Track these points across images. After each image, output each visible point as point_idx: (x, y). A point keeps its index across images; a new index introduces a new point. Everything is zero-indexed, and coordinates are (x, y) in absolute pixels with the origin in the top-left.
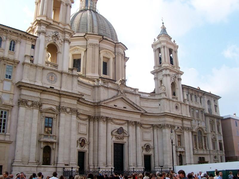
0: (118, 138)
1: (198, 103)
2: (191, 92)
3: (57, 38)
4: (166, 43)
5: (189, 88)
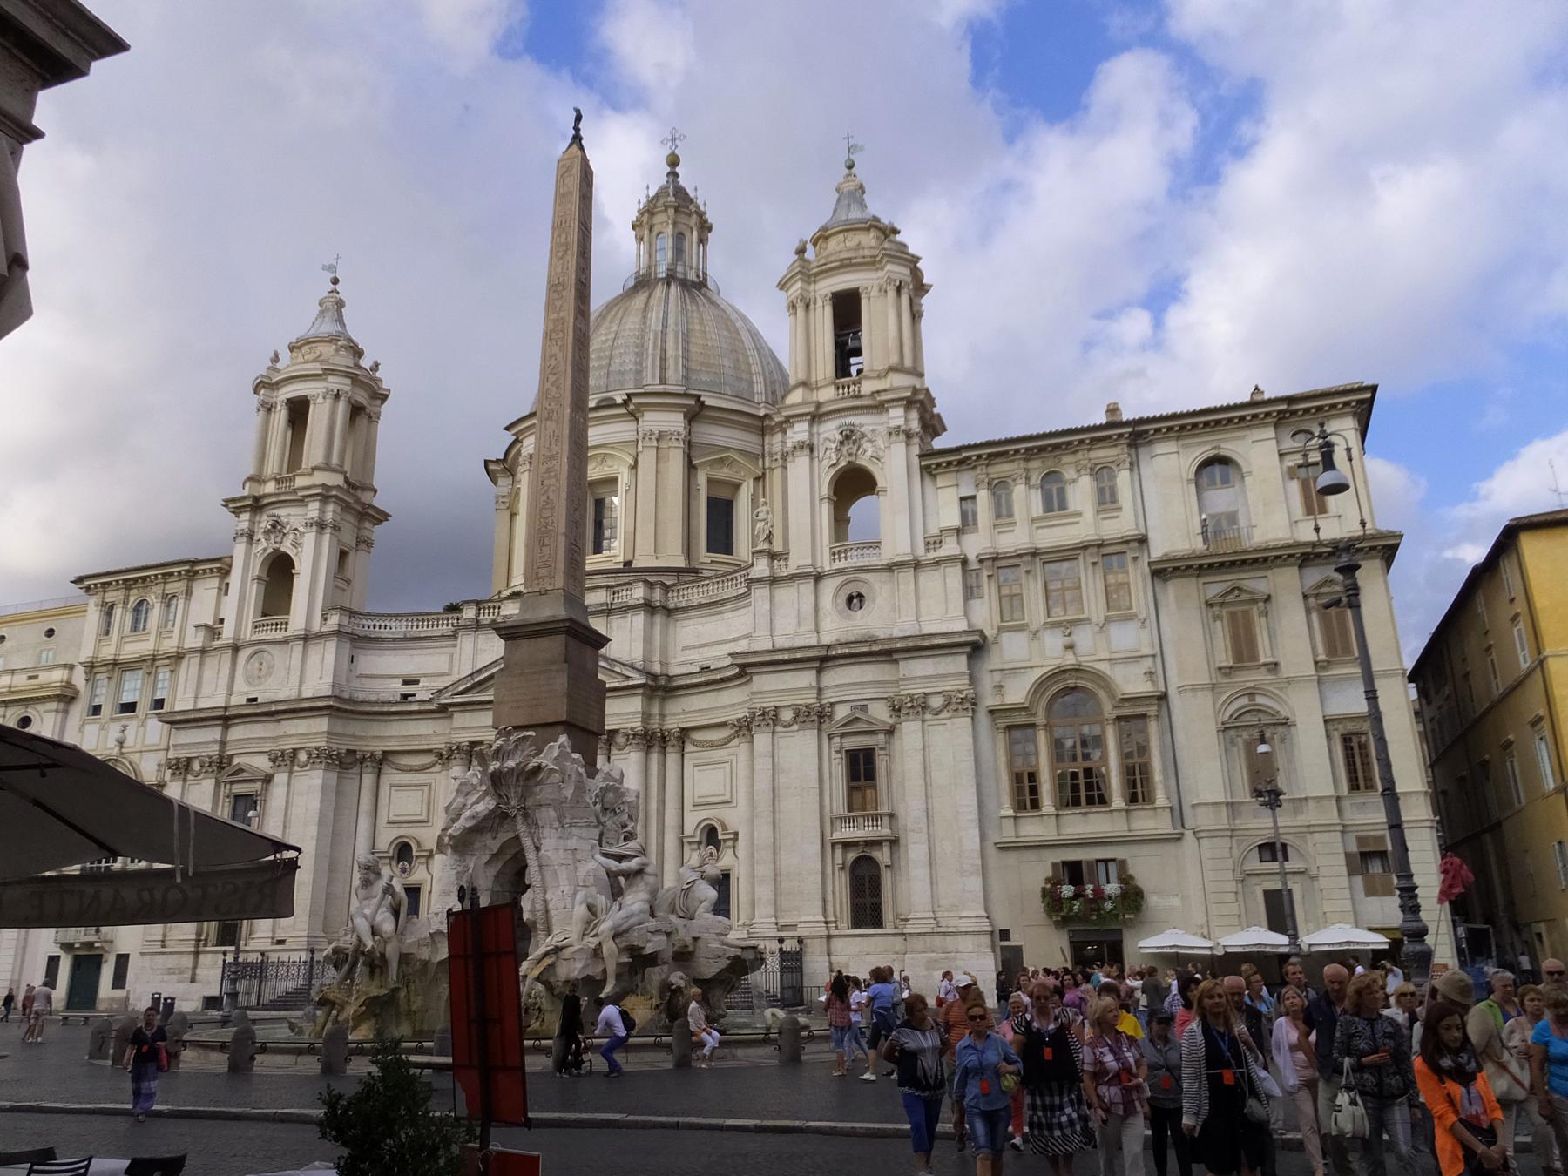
1: (1079, 514)
2: (1001, 469)
3: (280, 531)
4: (799, 284)
5: (969, 458)
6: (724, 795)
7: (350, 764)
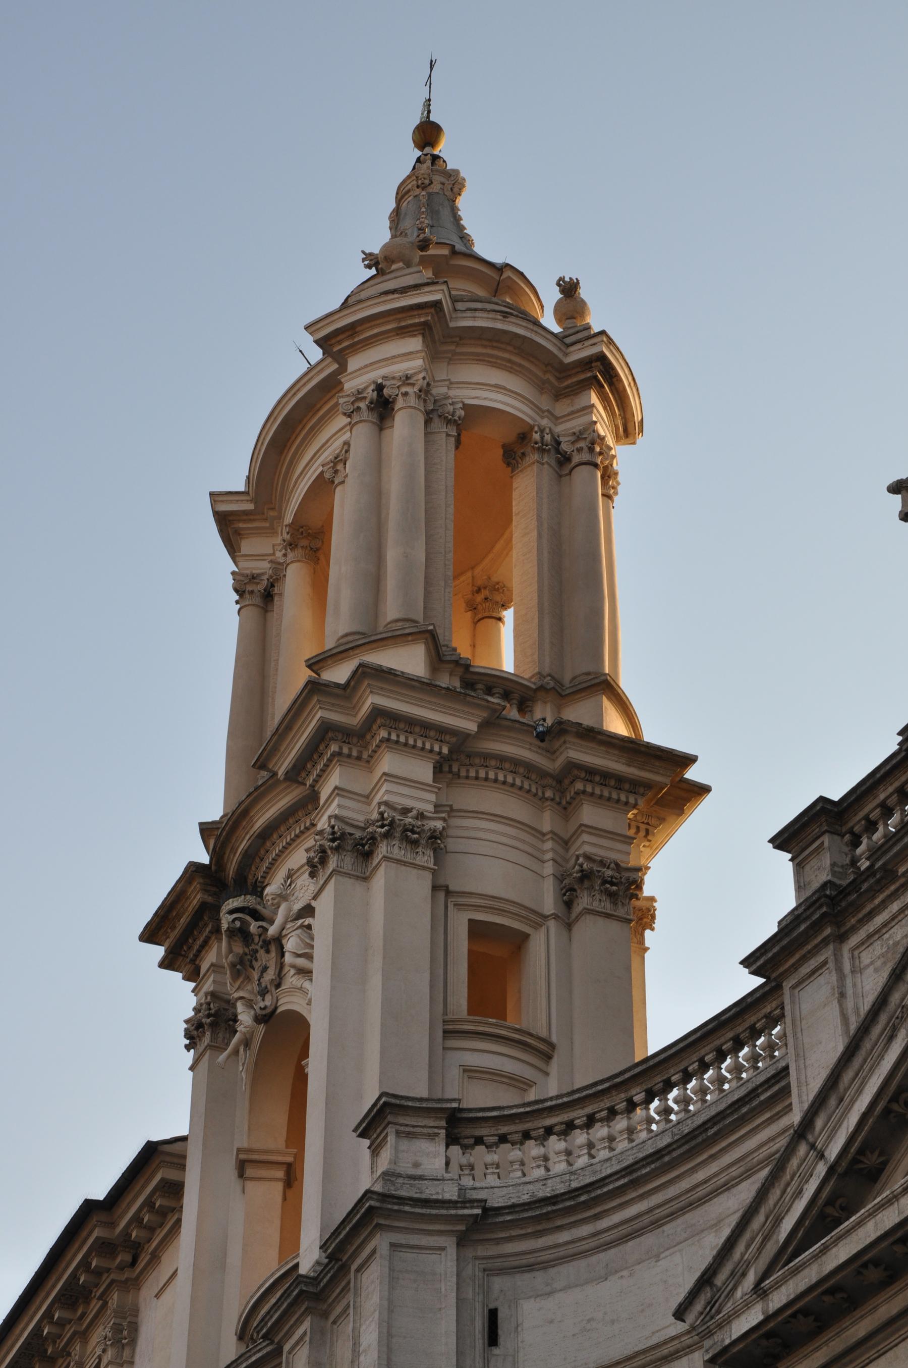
3: (266, 945)
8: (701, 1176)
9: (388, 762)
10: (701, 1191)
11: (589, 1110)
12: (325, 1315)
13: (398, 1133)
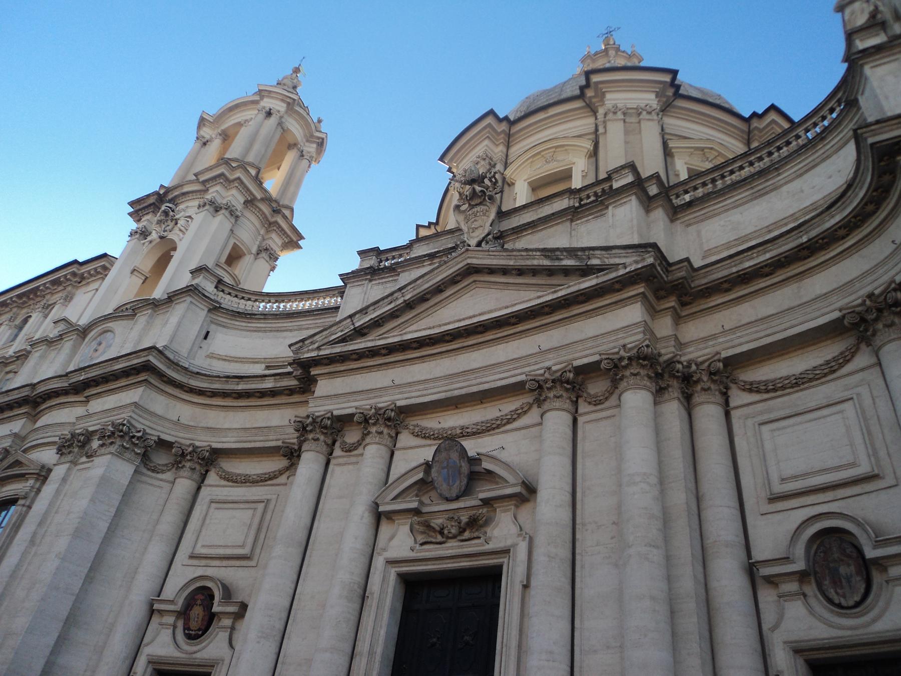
0: (441, 532)
3: (172, 220)
6: (853, 465)
7: (163, 465)
8: (285, 325)
9: (234, 192)
10: (283, 329)
11: (257, 298)
12: (155, 312)
13: (204, 277)
